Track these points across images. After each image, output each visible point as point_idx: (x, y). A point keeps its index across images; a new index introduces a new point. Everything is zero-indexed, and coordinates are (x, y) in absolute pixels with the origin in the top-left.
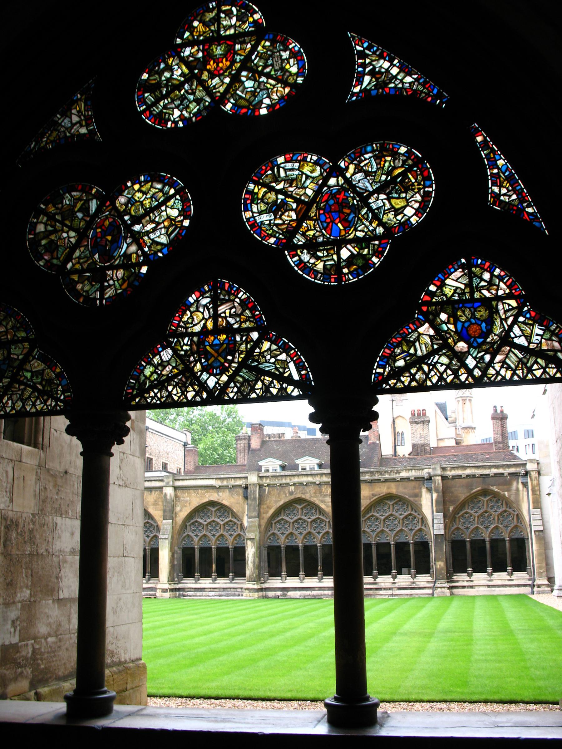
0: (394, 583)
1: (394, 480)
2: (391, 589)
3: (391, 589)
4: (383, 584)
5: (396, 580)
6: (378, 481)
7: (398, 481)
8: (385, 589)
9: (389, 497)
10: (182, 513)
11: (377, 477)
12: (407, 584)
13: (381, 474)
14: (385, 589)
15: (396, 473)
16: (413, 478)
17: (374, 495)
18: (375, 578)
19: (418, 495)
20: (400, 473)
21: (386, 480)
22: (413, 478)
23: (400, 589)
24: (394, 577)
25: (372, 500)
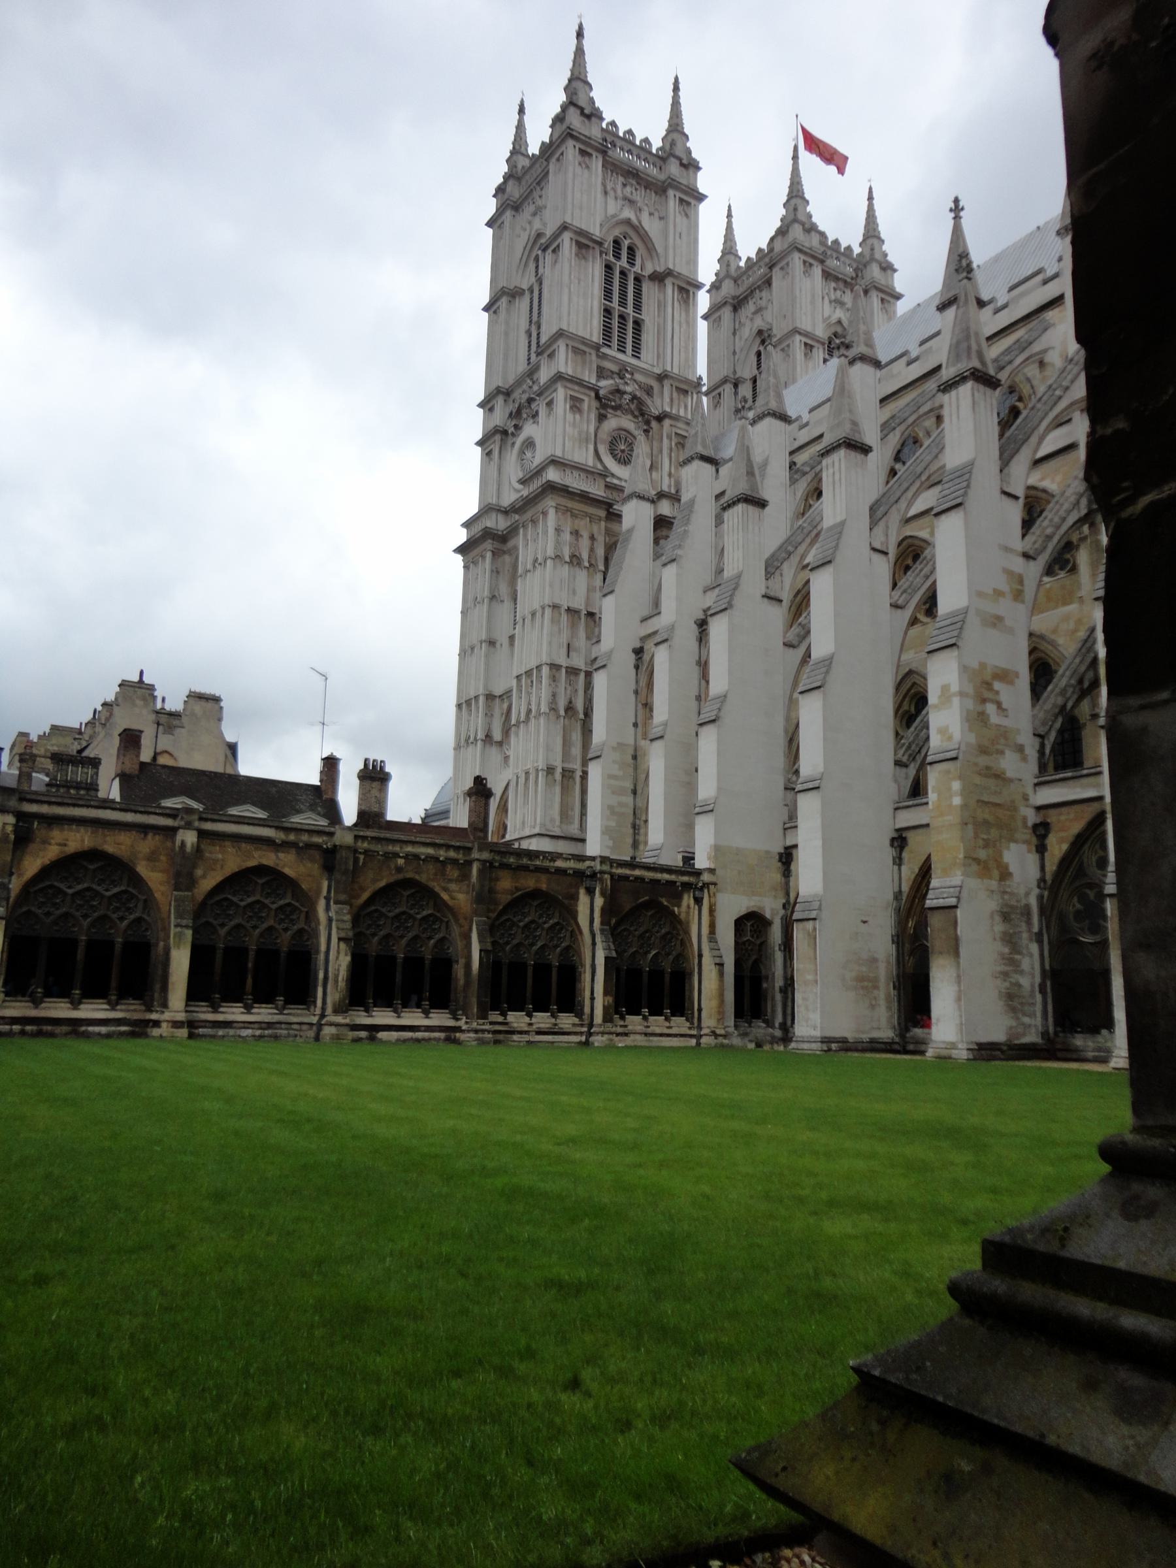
0: (530, 1024)
1: (545, 870)
2: (526, 1032)
3: (526, 1032)
4: (515, 1025)
5: (534, 1020)
6: (525, 868)
7: (551, 873)
8: (521, 1033)
9: (535, 894)
10: (207, 883)
11: (525, 861)
12: (548, 1026)
13: (530, 859)
14: (521, 1033)
15: (550, 861)
16: (571, 872)
17: (517, 889)
18: (504, 1014)
19: (575, 898)
20: (555, 861)
21: (538, 869)
22: (571, 872)
23: (539, 1033)
24: (530, 1015)
25: (515, 896)
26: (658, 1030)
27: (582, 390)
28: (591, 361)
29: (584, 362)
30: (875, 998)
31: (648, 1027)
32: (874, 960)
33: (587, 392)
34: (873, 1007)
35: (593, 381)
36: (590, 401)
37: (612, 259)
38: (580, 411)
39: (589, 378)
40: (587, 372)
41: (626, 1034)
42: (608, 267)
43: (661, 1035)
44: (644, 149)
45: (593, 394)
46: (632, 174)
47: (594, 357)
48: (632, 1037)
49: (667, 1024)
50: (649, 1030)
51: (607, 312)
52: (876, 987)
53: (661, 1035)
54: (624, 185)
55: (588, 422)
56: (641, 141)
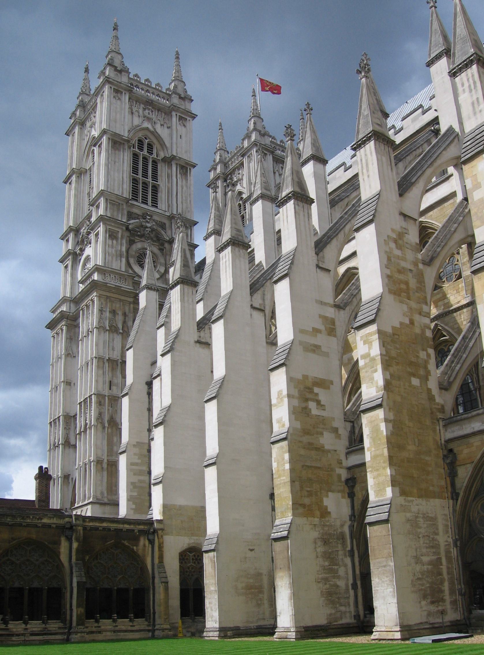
26: (124, 628)
27: (117, 226)
28: (123, 209)
29: (118, 210)
30: (261, 599)
31: (117, 626)
32: (260, 575)
33: (121, 227)
34: (259, 605)
35: (125, 221)
36: (123, 231)
37: (137, 150)
38: (116, 238)
39: (122, 218)
40: (120, 216)
41: (100, 632)
42: (135, 156)
43: (126, 631)
44: (158, 91)
45: (124, 228)
46: (149, 104)
47: (125, 207)
48: (104, 633)
49: (131, 624)
50: (117, 628)
51: (135, 181)
52: (261, 592)
53: (126, 631)
54: (144, 109)
55: (121, 245)
56: (156, 85)
